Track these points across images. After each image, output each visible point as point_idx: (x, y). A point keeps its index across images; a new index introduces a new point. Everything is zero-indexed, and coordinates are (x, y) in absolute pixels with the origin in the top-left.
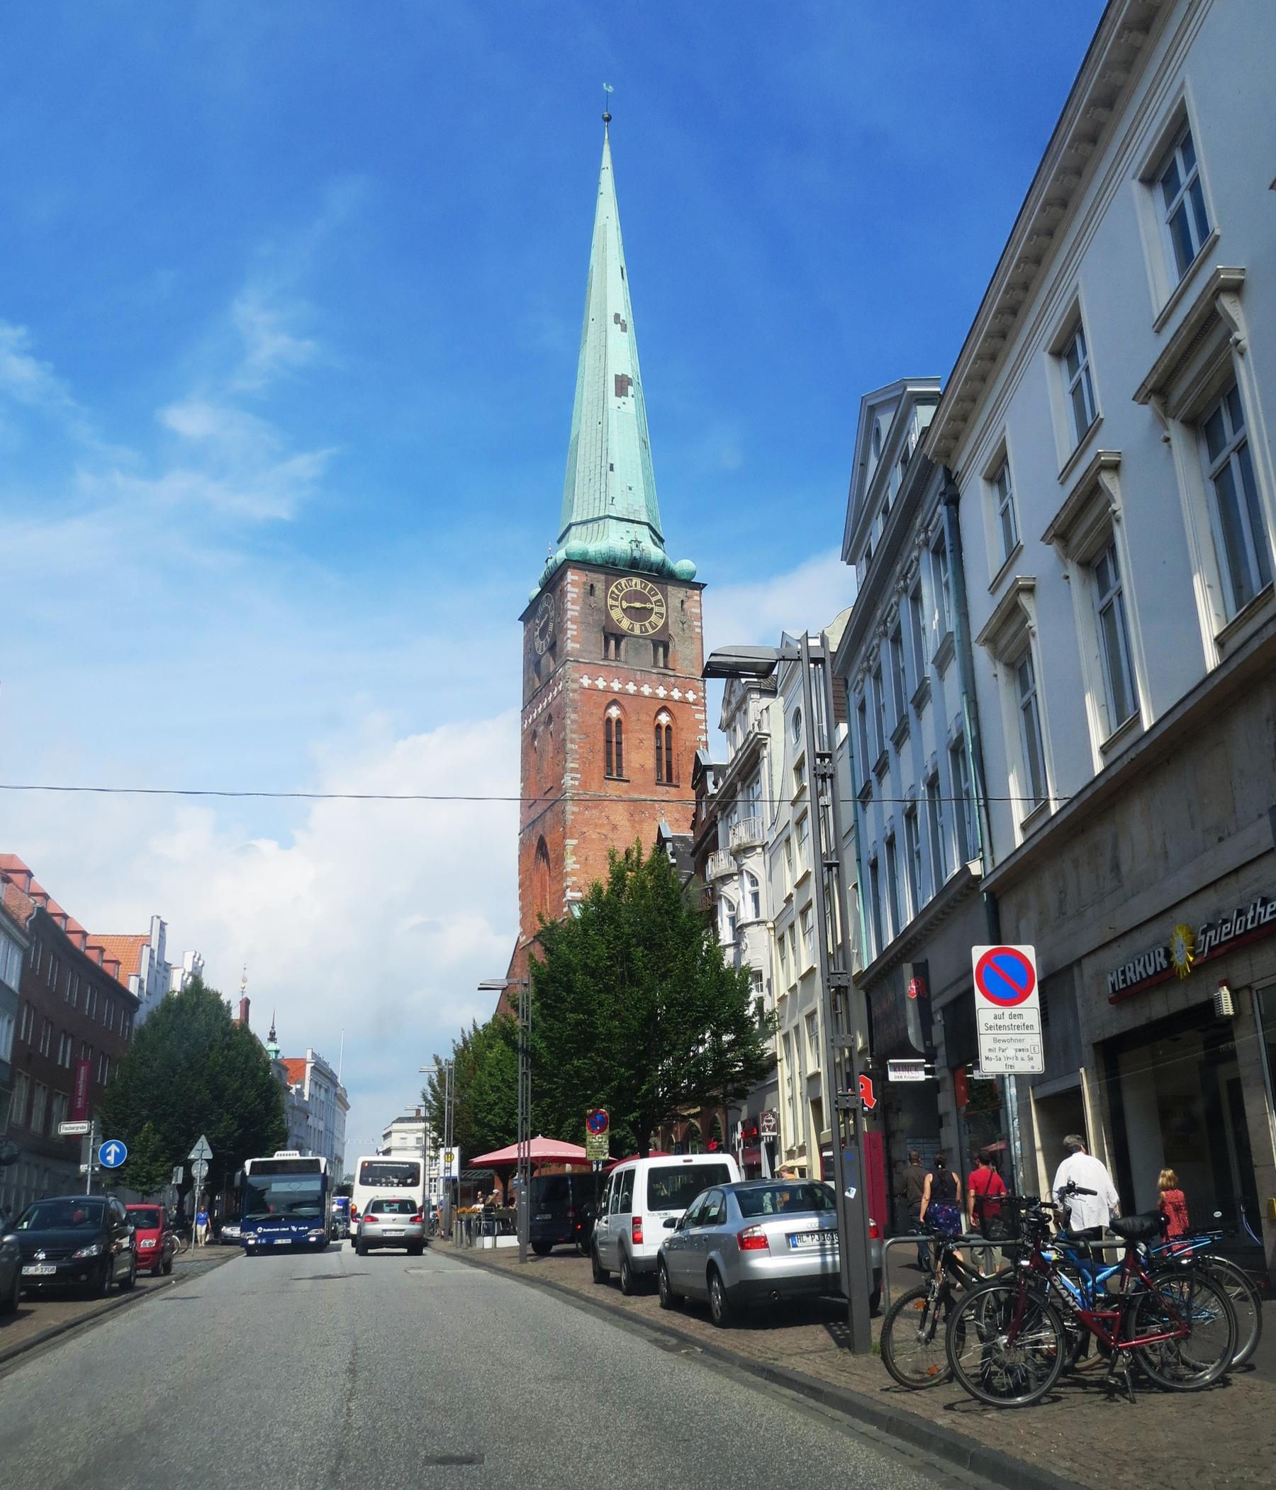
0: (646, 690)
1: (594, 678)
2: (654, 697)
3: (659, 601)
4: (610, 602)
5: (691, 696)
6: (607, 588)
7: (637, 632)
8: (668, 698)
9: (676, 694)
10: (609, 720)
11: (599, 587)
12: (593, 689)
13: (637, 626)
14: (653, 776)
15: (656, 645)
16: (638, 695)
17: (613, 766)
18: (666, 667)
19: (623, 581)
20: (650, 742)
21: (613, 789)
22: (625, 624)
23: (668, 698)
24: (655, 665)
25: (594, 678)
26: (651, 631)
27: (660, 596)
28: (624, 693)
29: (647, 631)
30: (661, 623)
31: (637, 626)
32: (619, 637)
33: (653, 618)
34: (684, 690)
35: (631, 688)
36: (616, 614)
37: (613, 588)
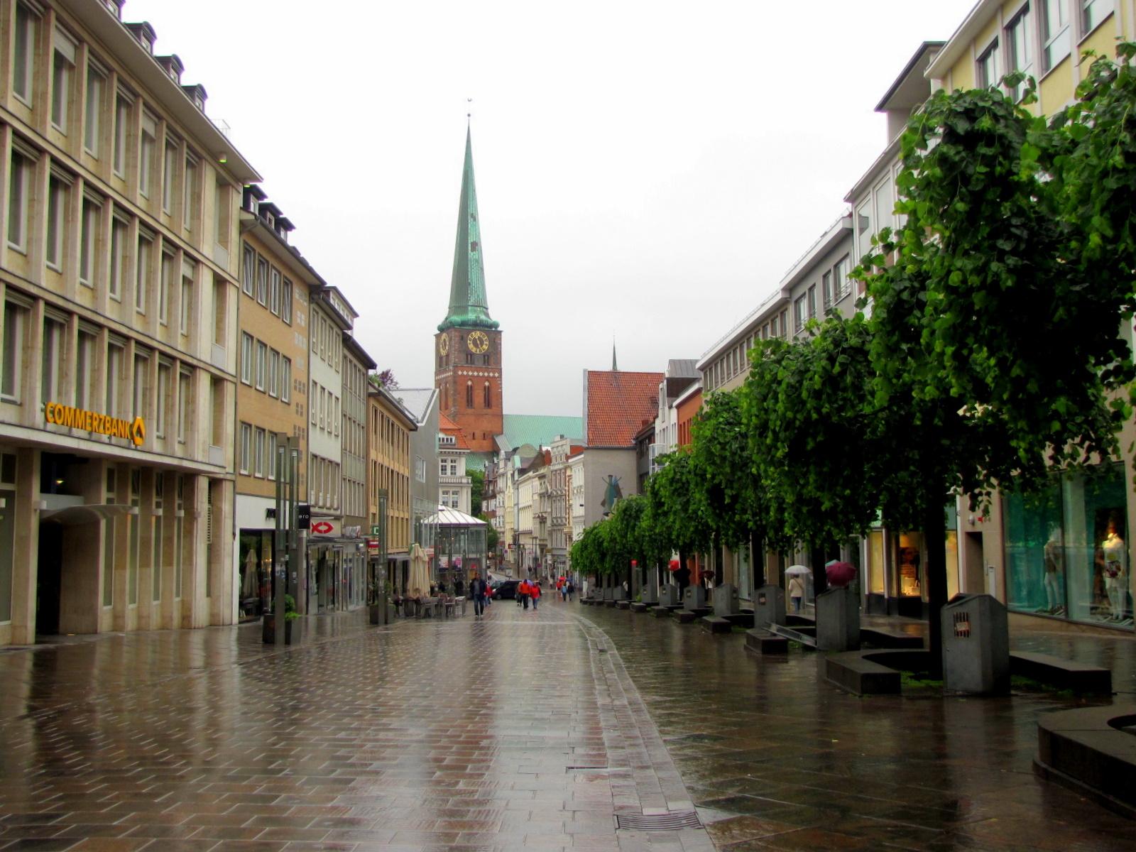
1: (462, 371)
2: (483, 376)
5: (497, 375)
7: (478, 352)
9: (491, 375)
11: (465, 336)
12: (462, 375)
14: (483, 405)
15: (484, 356)
17: (470, 402)
21: (470, 411)
22: (474, 350)
25: (462, 371)
28: (473, 376)
32: (472, 354)
33: (484, 346)
34: (494, 373)
36: (471, 346)
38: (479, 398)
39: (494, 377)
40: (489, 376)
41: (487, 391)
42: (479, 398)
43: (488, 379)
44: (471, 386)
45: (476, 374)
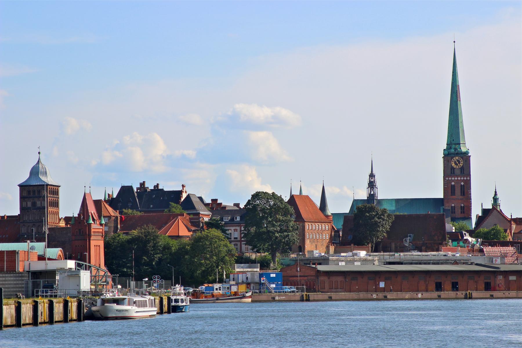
0: (459, 179)
2: (461, 180)
16: (458, 180)
20: (460, 188)
23: (464, 179)
28: (455, 180)
32: (454, 169)
36: (453, 165)
38: (458, 191)
39: (467, 179)
40: (464, 179)
43: (463, 181)
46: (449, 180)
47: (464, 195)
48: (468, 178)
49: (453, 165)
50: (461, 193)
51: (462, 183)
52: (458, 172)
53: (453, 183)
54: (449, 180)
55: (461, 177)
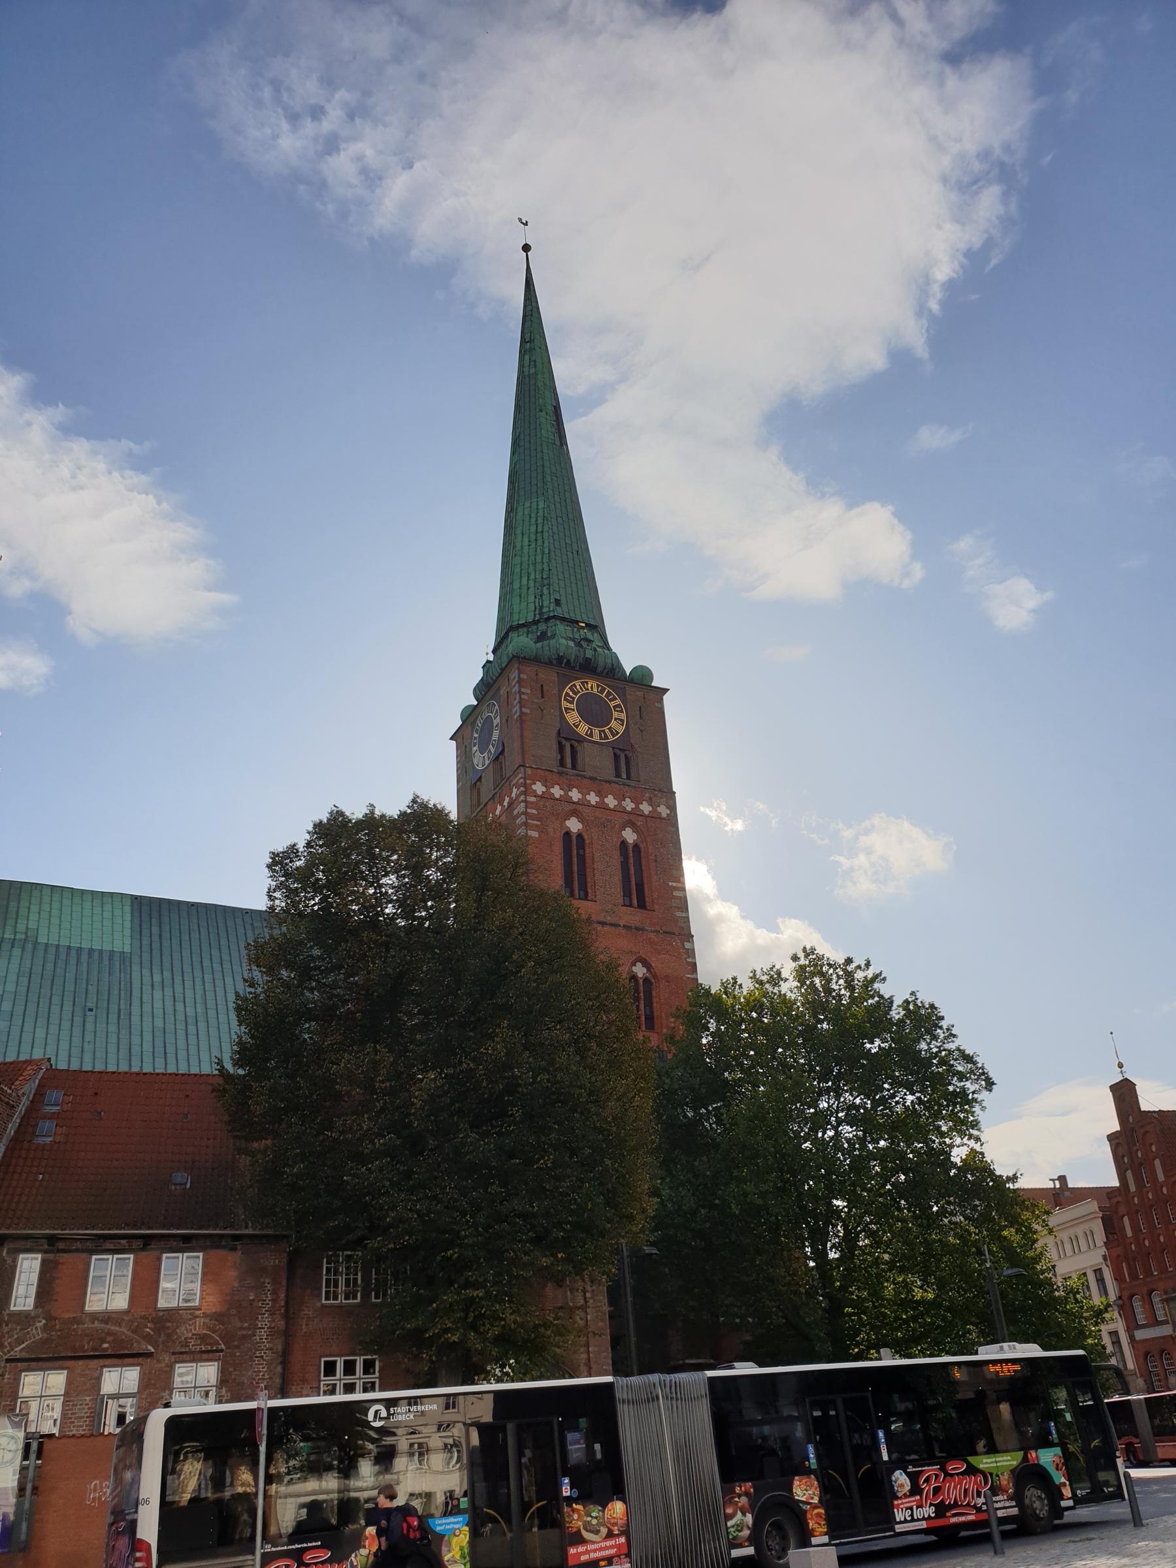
0: (611, 801)
3: (619, 706)
4: (564, 704)
6: (561, 692)
7: (596, 738)
8: (636, 812)
10: (568, 834)
13: (596, 731)
18: (629, 777)
19: (578, 683)
20: (616, 860)
22: (583, 729)
23: (636, 812)
24: (618, 775)
26: (611, 739)
27: (618, 702)
28: (584, 803)
29: (606, 738)
30: (621, 730)
31: (596, 731)
33: (613, 724)
35: (593, 798)
36: (573, 718)
37: (567, 690)
39: (654, 816)
41: (632, 857)
42: (606, 874)
44: (580, 836)
45: (593, 798)
46: (547, 797)
47: (642, 905)
48: (663, 811)
49: (573, 718)
50: (627, 893)
51: (630, 836)
52: (598, 762)
53: (574, 825)
54: (547, 797)
55: (621, 798)
